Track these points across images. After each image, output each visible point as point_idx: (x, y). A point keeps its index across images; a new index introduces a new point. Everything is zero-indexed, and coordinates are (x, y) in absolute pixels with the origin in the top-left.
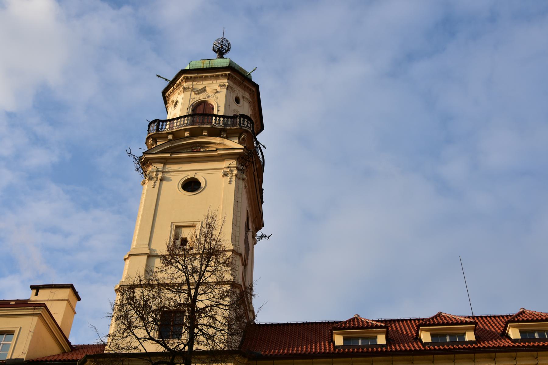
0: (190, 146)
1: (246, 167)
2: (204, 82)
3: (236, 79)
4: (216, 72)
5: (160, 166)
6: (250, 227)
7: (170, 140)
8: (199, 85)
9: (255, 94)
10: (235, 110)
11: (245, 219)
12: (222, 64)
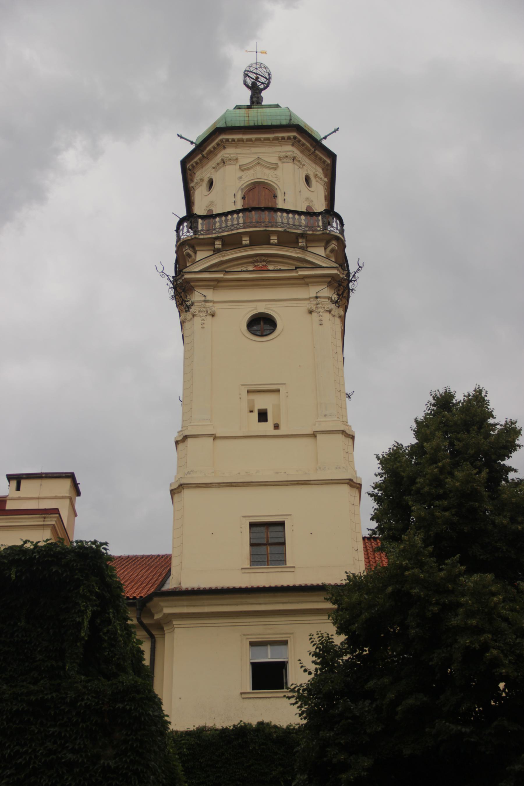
3: (303, 145)
4: (274, 133)
5: (210, 294)
8: (246, 155)
9: (330, 168)
10: (307, 199)
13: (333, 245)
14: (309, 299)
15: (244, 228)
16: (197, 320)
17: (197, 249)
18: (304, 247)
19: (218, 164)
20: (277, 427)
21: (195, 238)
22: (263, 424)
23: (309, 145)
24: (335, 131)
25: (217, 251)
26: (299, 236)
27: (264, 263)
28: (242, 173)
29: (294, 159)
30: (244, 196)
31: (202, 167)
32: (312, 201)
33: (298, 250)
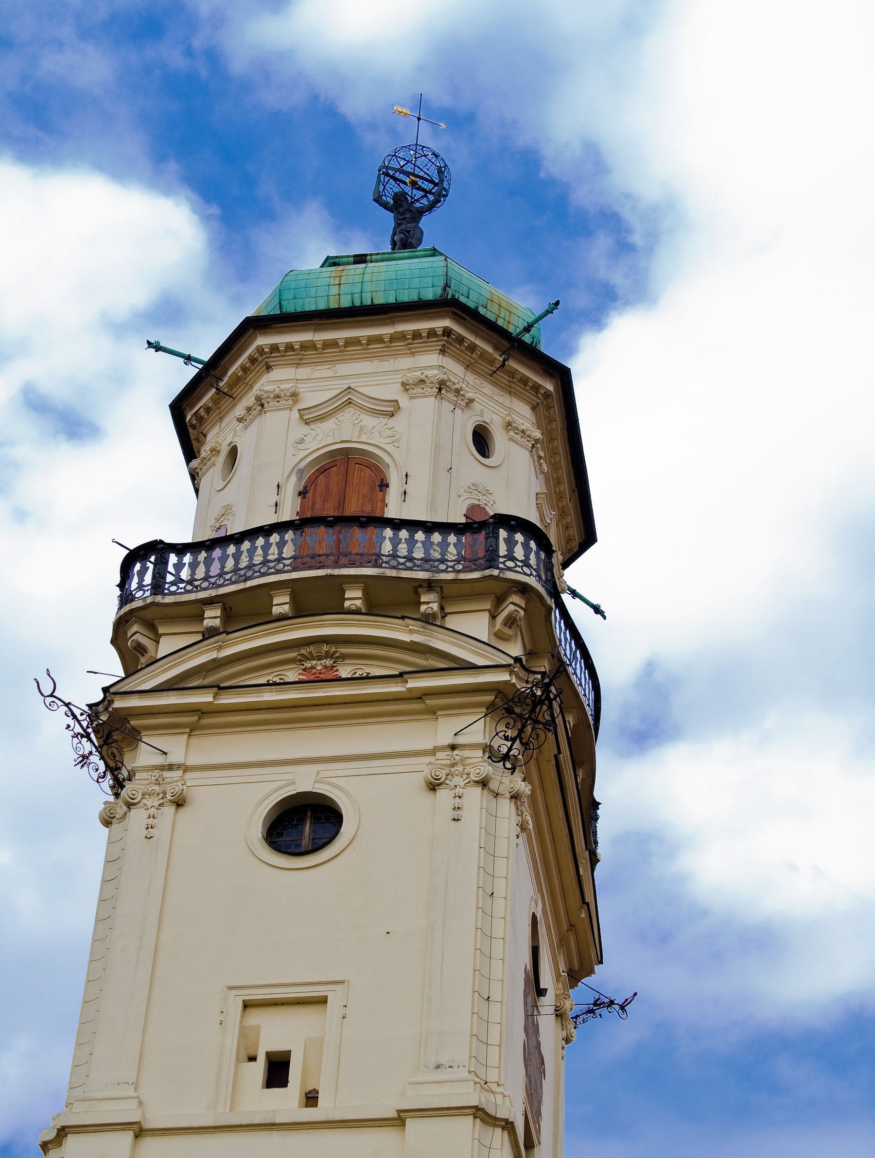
0: (293, 655)
1: (525, 745)
2: (344, 369)
3: (472, 348)
5: (176, 748)
6: (547, 980)
7: (210, 633)
10: (474, 488)
11: (526, 958)
12: (416, 283)
13: (512, 607)
14: (434, 751)
15: (295, 569)
16: (138, 816)
17: (161, 631)
18: (434, 616)
19: (249, 409)
20: (311, 1099)
21: (153, 604)
22: (276, 1092)
23: (489, 349)
24: (549, 312)
25: (210, 633)
26: (421, 586)
27: (329, 662)
28: (306, 429)
29: (442, 386)
30: (305, 487)
31: (221, 419)
32: (488, 492)
33: (413, 625)
